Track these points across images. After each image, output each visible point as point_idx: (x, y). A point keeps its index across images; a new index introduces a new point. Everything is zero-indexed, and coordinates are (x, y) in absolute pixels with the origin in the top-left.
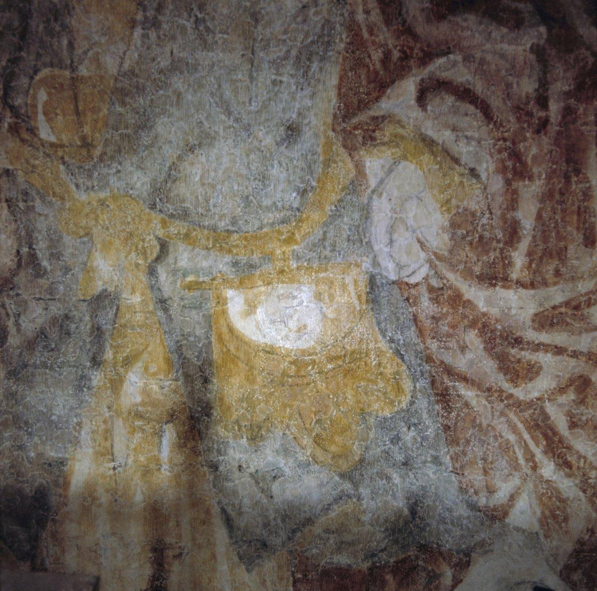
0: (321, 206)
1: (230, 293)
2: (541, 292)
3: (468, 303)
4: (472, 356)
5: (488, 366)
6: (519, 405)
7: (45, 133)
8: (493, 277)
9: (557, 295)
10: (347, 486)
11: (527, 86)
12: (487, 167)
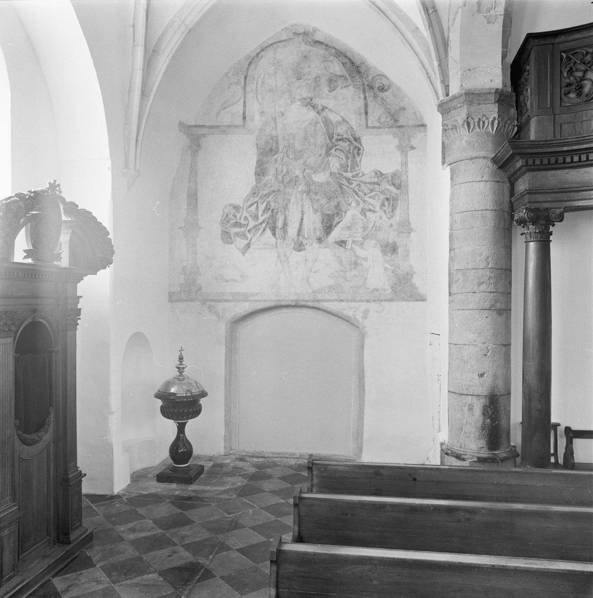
0: (324, 163)
1: (313, 175)
2: (352, 173)
3: (343, 175)
4: (344, 182)
5: (346, 183)
6: (351, 188)
7: (291, 157)
8: (346, 171)
9: (354, 173)
10: (329, 201)
11: (348, 149)
12: (344, 158)
